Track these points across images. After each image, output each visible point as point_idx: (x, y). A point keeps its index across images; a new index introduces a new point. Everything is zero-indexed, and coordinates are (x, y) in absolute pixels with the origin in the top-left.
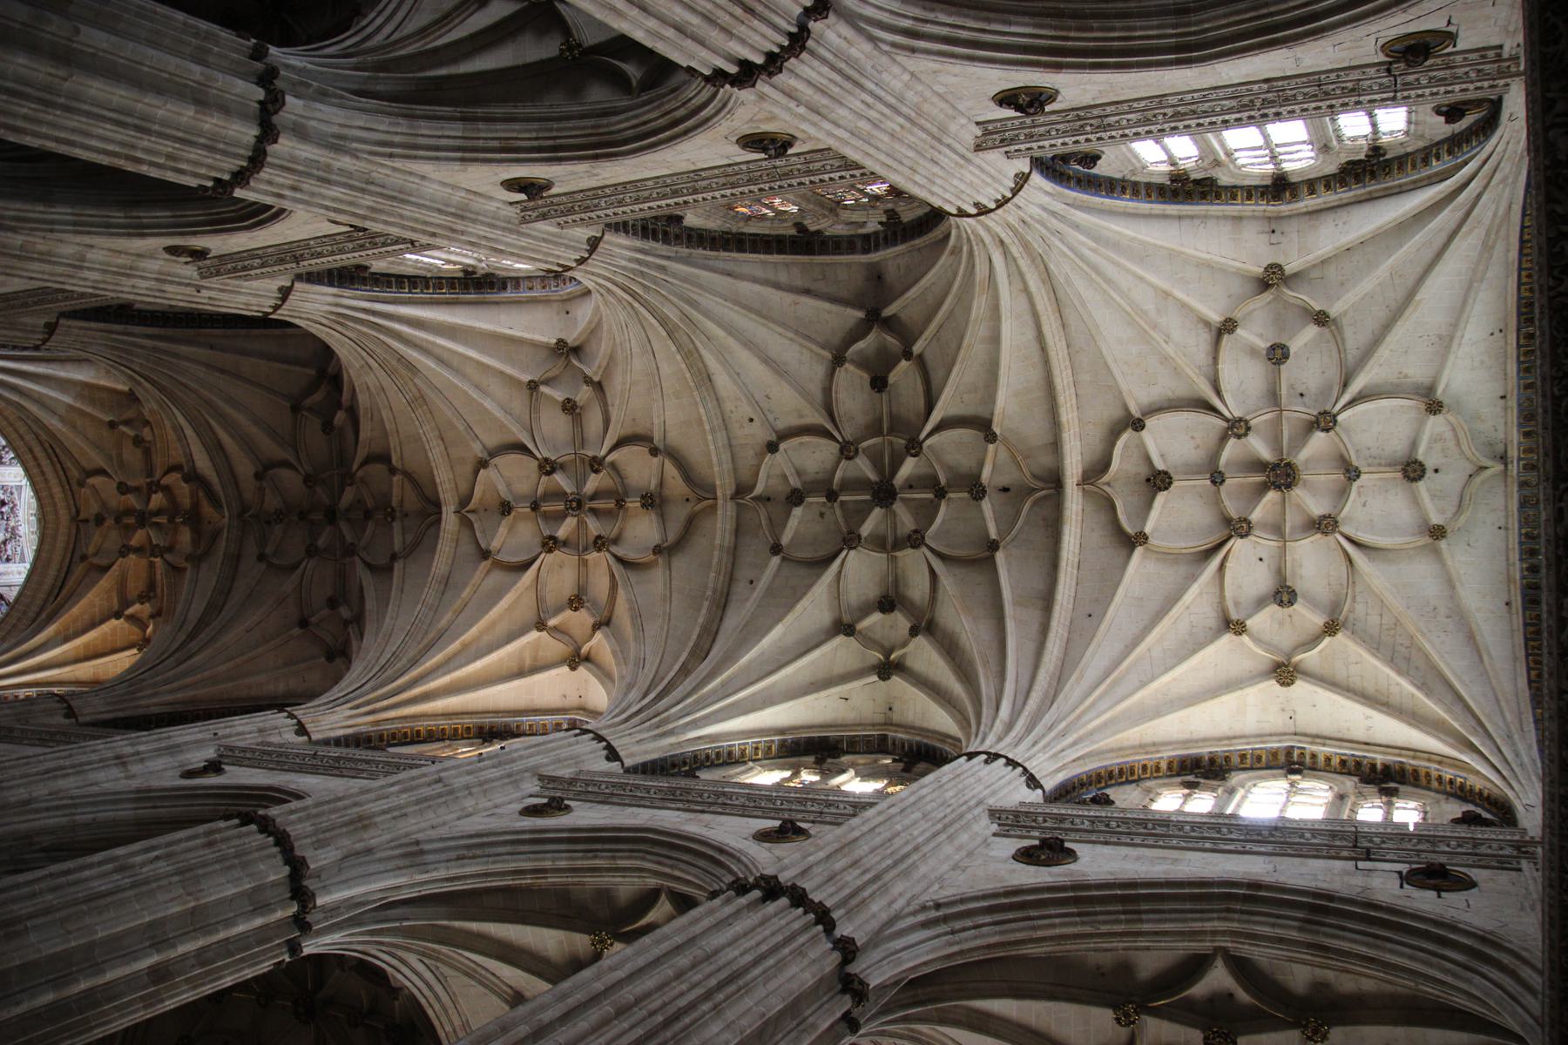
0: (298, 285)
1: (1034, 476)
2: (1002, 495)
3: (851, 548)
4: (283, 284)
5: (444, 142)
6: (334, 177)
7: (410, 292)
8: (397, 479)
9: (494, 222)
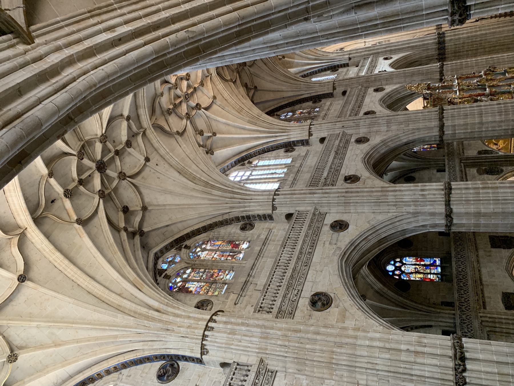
0: (308, 138)
1: (46, 217)
2: (53, 199)
3: (103, 135)
4: (313, 137)
5: (384, 230)
6: (412, 203)
7: (264, 148)
8: (229, 78)
9: (329, 205)
